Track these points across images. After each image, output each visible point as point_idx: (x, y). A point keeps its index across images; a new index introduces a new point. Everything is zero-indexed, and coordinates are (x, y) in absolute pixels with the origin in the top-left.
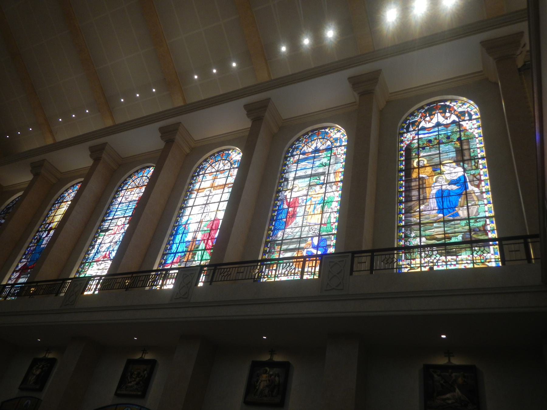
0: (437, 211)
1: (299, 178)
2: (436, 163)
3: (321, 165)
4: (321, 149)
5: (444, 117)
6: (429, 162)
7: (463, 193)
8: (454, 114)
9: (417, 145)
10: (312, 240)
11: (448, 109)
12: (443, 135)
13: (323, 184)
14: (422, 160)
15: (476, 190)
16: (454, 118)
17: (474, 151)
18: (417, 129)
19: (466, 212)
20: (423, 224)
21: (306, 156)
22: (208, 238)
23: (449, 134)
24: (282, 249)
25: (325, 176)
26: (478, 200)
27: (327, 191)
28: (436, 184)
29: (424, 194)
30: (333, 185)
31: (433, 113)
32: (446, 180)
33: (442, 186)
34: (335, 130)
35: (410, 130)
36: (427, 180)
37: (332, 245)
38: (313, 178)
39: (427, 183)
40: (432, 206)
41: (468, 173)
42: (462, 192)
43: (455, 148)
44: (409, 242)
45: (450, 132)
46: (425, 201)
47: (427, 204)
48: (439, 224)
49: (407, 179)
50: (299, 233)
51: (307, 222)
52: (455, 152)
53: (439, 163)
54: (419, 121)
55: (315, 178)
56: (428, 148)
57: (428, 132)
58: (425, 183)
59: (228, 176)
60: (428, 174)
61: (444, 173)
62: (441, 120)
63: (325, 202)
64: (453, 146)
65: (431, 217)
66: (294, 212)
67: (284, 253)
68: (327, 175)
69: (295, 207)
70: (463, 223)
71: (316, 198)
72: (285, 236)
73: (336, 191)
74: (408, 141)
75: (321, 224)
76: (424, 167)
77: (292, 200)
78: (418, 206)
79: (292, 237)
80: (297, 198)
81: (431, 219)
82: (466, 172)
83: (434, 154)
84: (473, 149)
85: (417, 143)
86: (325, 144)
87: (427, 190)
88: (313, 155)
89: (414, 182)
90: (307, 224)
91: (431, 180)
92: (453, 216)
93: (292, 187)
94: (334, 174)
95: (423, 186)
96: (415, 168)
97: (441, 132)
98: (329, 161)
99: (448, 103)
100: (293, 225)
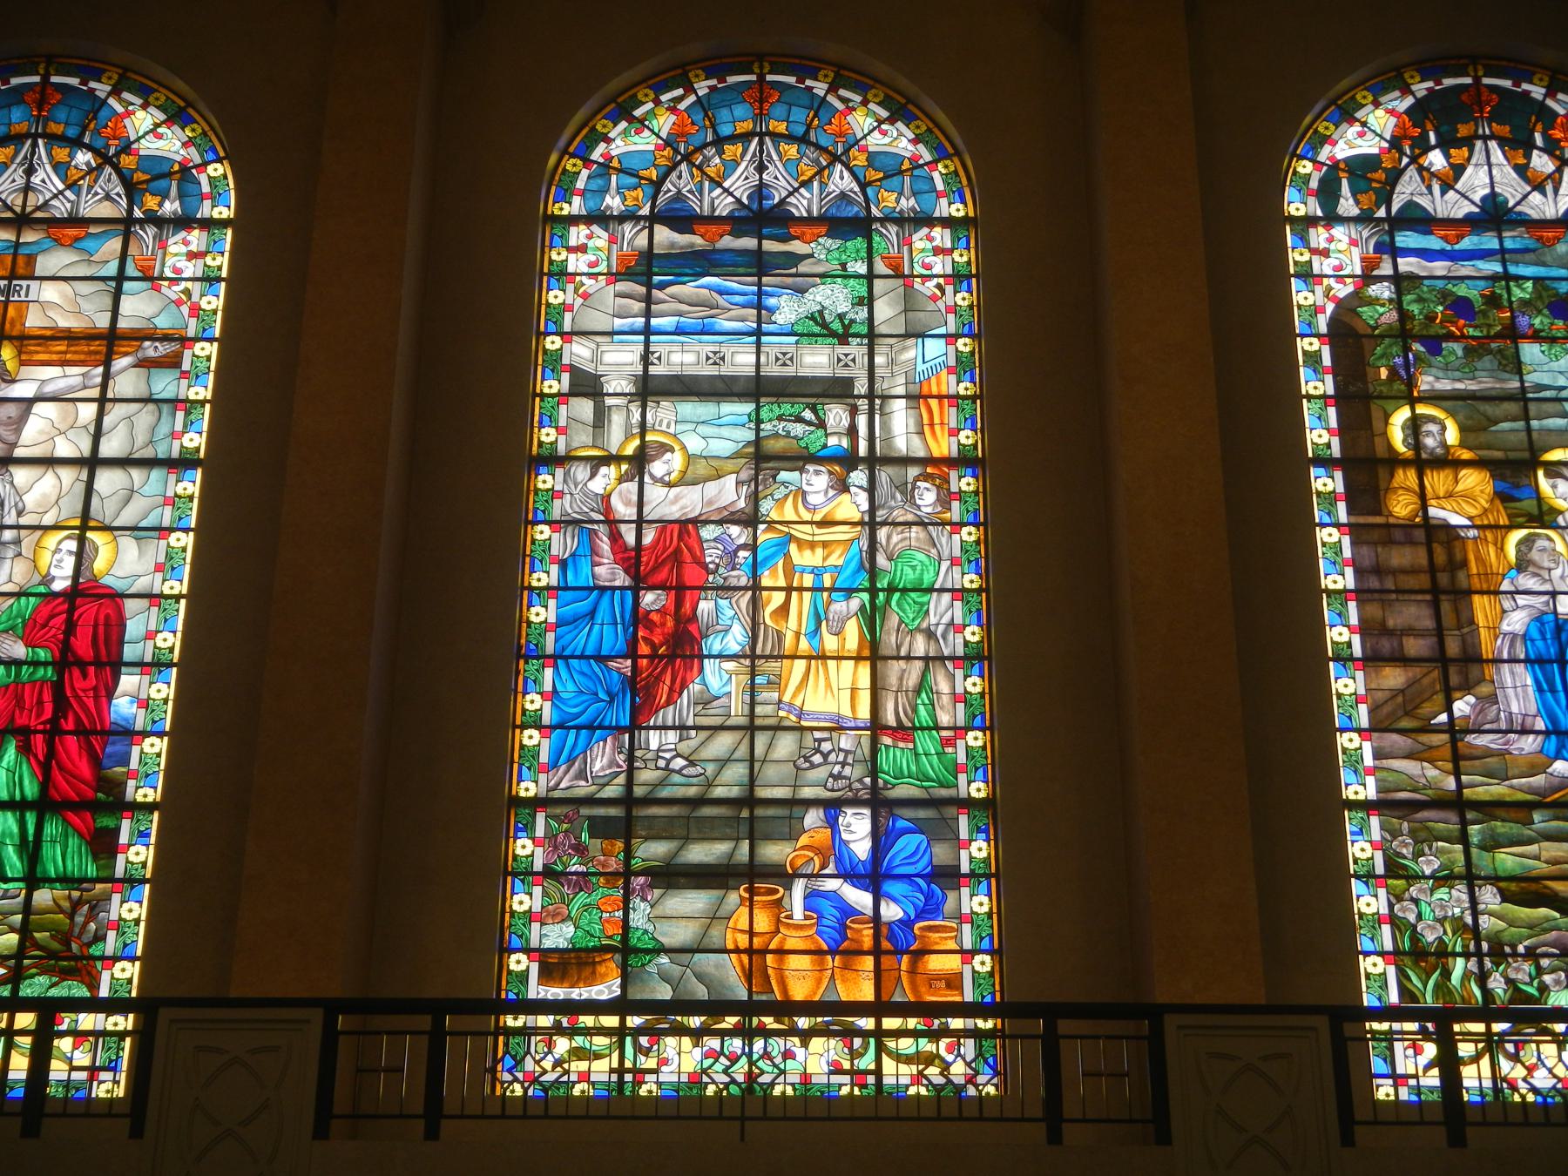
0: (1540, 738)
1: (676, 387)
2: (1512, 455)
3: (817, 329)
4: (797, 214)
5: (1522, 170)
6: (1472, 437)
9: (1395, 315)
10: (832, 824)
11: (1539, 127)
12: (1529, 284)
13: (849, 460)
14: (1432, 419)
18: (1382, 213)
20: (1478, 805)
21: (697, 241)
22: (54, 721)
24: (636, 863)
25: (854, 411)
27: (881, 515)
29: (1465, 630)
30: (917, 479)
31: (1463, 130)
33: (1554, 594)
34: (870, 96)
35: (1341, 211)
36: (1470, 546)
37: (965, 868)
38: (777, 412)
40: (1515, 709)
44: (1416, 901)
46: (1474, 670)
47: (1484, 689)
48: (1557, 819)
49: (1361, 520)
50: (737, 772)
51: (780, 701)
53: (1526, 455)
54: (1387, 164)
55: (787, 409)
56: (1458, 348)
57: (1449, 248)
58: (1464, 564)
59: (121, 277)
60: (1473, 512)
61: (1561, 521)
62: (1510, 187)
63: (883, 583)
65: (1516, 771)
66: (677, 615)
67: (652, 887)
68: (863, 404)
69: (680, 591)
71: (819, 551)
72: (646, 776)
73: (943, 524)
74: (1340, 279)
75: (876, 726)
76: (1446, 461)
77: (649, 537)
78: (1440, 698)
79: (692, 792)
80: (687, 527)
81: (1515, 781)
83: (1494, 393)
85: (1390, 301)
86: (816, 184)
87: (1481, 606)
88: (749, 243)
89: (1400, 543)
90: (782, 713)
91: (1492, 550)
93: (637, 442)
94: (913, 403)
95: (1453, 578)
97: (1517, 263)
98: (863, 314)
99: (1537, 92)
100: (684, 707)
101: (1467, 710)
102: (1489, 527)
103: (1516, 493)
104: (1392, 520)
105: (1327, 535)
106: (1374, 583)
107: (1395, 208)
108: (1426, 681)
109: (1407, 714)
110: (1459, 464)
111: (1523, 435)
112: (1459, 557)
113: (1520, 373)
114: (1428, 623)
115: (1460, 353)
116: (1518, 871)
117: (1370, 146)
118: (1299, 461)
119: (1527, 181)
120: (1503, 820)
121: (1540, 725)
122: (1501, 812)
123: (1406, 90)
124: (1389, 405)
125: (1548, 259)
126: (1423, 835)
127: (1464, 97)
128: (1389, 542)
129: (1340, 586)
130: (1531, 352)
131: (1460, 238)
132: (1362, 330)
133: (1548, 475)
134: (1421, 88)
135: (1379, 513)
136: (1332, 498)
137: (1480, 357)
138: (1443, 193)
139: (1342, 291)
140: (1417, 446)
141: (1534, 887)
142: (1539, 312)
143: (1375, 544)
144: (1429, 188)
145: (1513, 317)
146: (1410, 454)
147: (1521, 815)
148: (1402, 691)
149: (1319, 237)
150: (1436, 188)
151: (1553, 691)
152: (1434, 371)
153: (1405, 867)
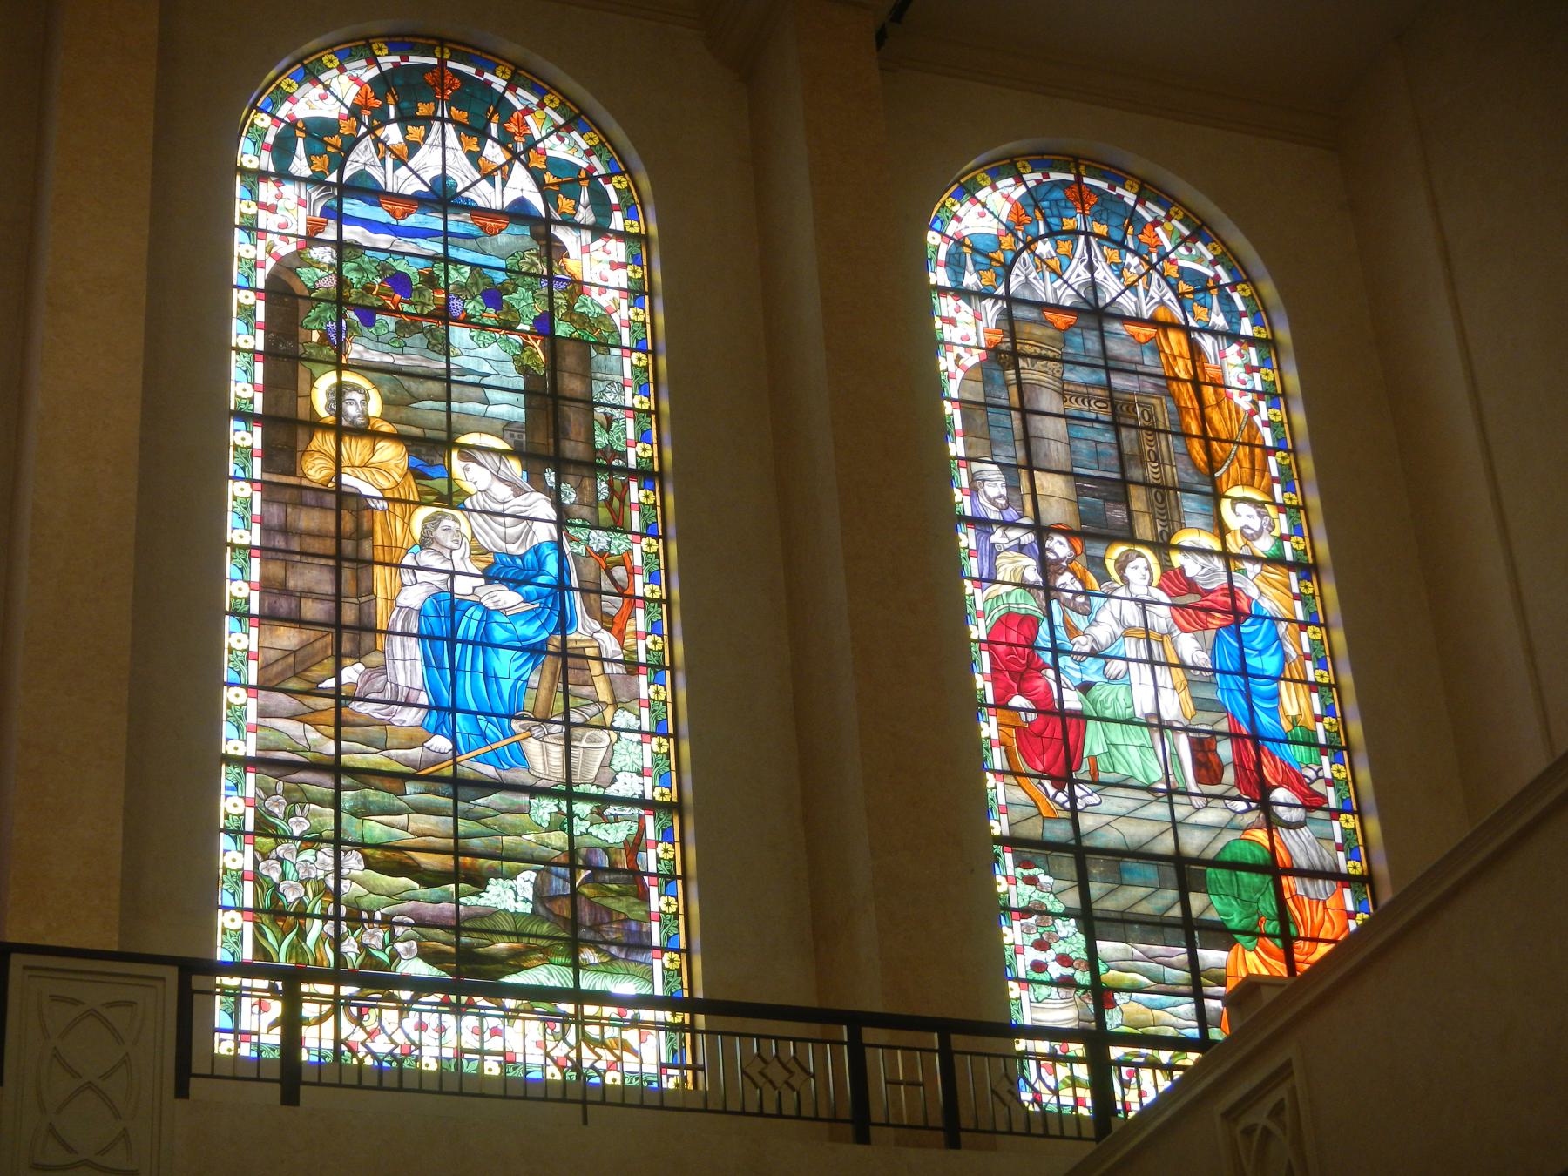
0: (423, 712)
2: (429, 434)
5: (474, 158)
6: (393, 411)
7: (551, 648)
8: (526, 165)
9: (333, 281)
11: (496, 118)
12: (467, 269)
14: (357, 388)
15: (609, 644)
16: (521, 185)
17: (610, 419)
19: (556, 752)
20: (354, 772)
23: (500, 277)
26: (616, 704)
28: (427, 559)
29: (363, 599)
31: (423, 109)
32: (477, 551)
33: (453, 574)
36: (378, 517)
39: (379, 541)
40: (401, 681)
41: (578, 541)
42: (545, 641)
43: (524, 370)
44: (281, 861)
45: (501, 263)
46: (367, 639)
47: (374, 659)
48: (429, 792)
49: (275, 478)
52: (522, 397)
53: (443, 435)
54: (345, 131)
56: (391, 321)
57: (394, 222)
60: (386, 484)
61: (468, 503)
62: (461, 172)
64: (516, 358)
65: (395, 742)
70: (545, 809)
74: (284, 236)
76: (365, 431)
78: (330, 663)
81: (392, 752)
82: (571, 530)
83: (419, 370)
84: (608, 410)
85: (331, 266)
92: (498, 759)
95: (358, 548)
96: (315, 425)
97: (458, 247)
99: (499, 84)
101: (355, 677)
102: (399, 501)
103: (429, 471)
104: (305, 483)
105: (237, 489)
106: (279, 542)
107: (347, 175)
108: (319, 645)
109: (295, 675)
110: (377, 435)
111: (443, 416)
112: (366, 526)
113: (448, 355)
114: (329, 589)
115: (392, 327)
116: (384, 840)
117: (330, 110)
118: (220, 413)
119: (478, 168)
120: (377, 789)
121: (423, 699)
122: (376, 781)
123: (372, 61)
124: (317, 369)
125: (488, 248)
126: (297, 796)
127: (428, 77)
128: (300, 504)
129: (245, 542)
130: (460, 335)
131: (406, 214)
132: (299, 289)
133: (462, 457)
134: (387, 61)
135: (294, 474)
136: (249, 452)
137: (411, 334)
138: (395, 168)
139: (286, 249)
140: (339, 413)
141: (398, 856)
142: (473, 298)
143: (286, 504)
144: (383, 160)
145: (448, 300)
146: (331, 420)
147: (395, 785)
148: (294, 652)
149: (267, 191)
150: (389, 162)
151: (440, 667)
152: (364, 341)
153: (275, 826)
